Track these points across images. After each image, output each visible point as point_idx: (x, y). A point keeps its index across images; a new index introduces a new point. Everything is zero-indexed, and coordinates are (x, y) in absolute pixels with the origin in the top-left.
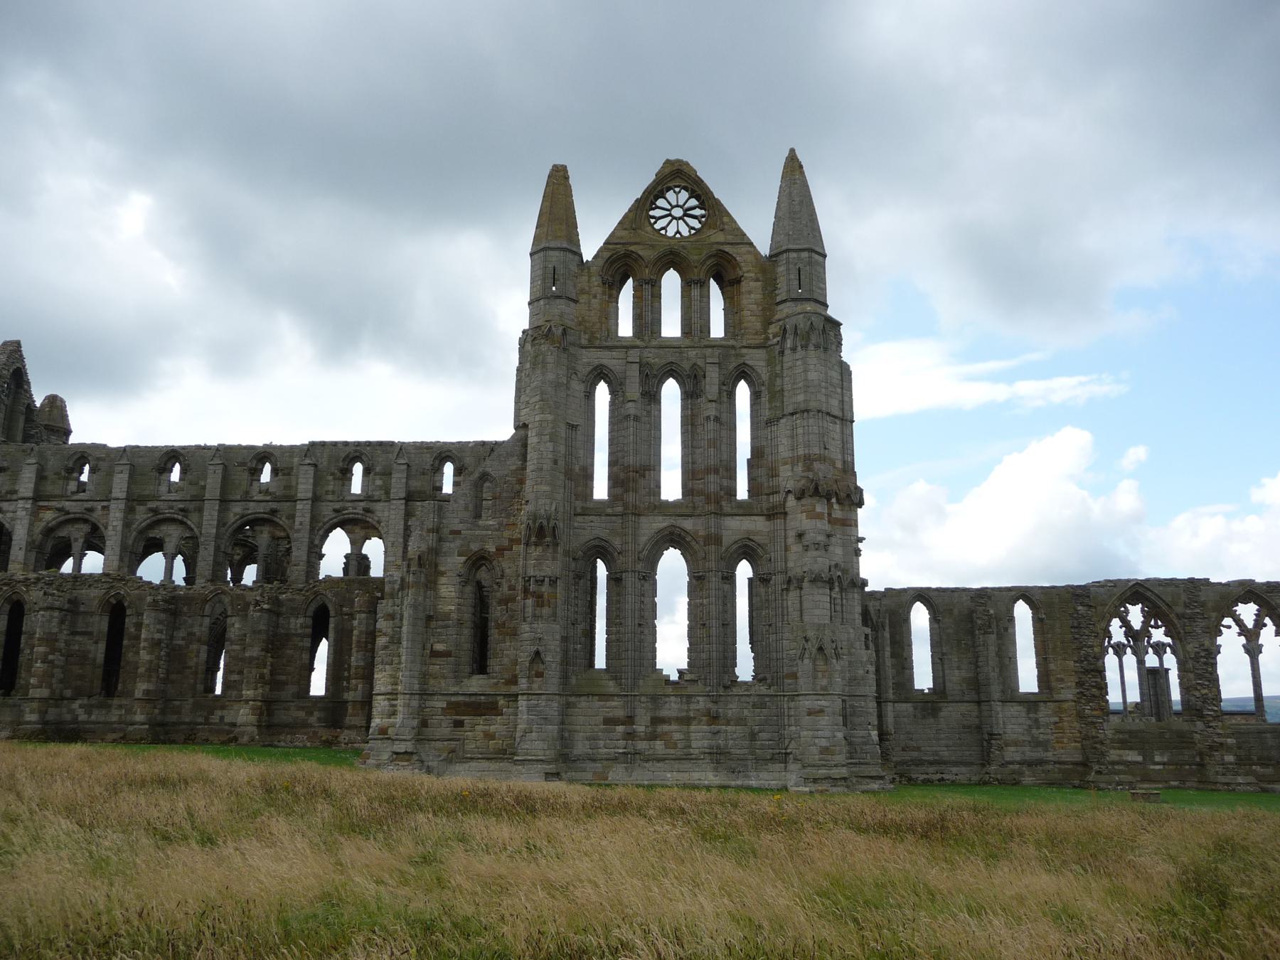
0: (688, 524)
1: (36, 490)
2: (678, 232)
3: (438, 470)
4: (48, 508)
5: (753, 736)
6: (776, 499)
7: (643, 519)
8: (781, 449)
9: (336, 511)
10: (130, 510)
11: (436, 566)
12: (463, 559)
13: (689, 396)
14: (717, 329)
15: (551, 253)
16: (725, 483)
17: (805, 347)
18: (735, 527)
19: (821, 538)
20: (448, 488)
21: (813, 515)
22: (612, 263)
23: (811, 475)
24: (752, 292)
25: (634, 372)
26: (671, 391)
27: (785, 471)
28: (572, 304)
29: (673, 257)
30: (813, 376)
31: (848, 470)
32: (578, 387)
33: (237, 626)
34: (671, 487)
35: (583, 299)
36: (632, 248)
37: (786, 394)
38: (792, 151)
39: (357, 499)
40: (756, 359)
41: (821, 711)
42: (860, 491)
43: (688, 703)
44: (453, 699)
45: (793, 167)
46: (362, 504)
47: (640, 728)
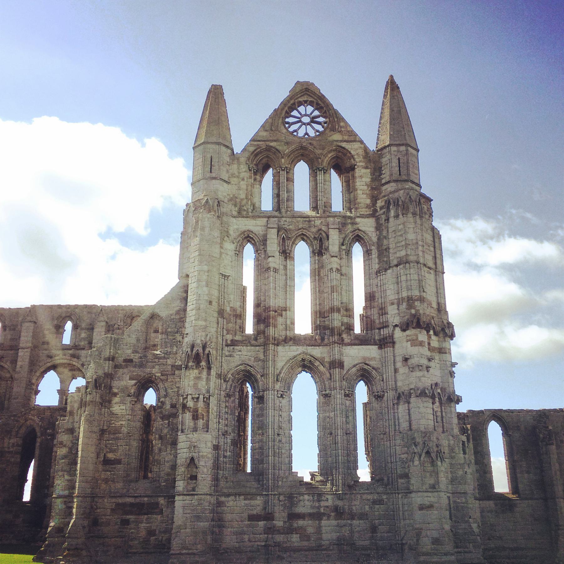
0: (317, 352)
2: (306, 134)
5: (374, 529)
6: (385, 332)
7: (280, 348)
8: (389, 292)
11: (111, 388)
12: (134, 382)
15: (209, 146)
16: (345, 320)
18: (353, 355)
19: (424, 362)
21: (415, 342)
22: (256, 155)
23: (413, 311)
24: (363, 177)
25: (273, 235)
27: (392, 310)
29: (304, 152)
30: (411, 236)
31: (441, 309)
32: (230, 247)
34: (303, 325)
35: (234, 180)
36: (272, 144)
37: (391, 251)
40: (367, 226)
41: (431, 507)
43: (319, 501)
44: (120, 501)
45: (392, 86)
47: (279, 523)
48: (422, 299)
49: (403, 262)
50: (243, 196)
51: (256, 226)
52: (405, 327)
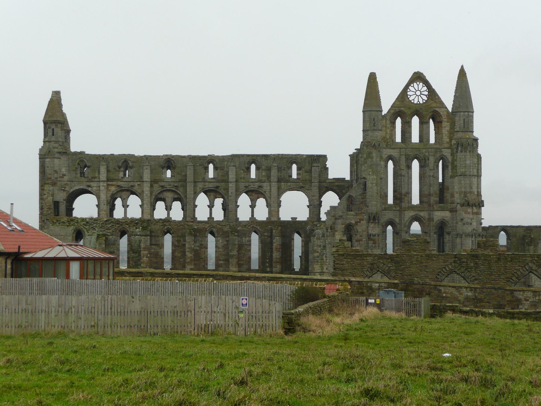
0: (422, 214)
1: (107, 177)
3: (290, 168)
4: (112, 185)
6: (454, 205)
7: (406, 212)
8: (456, 187)
9: (246, 187)
10: (152, 186)
13: (422, 167)
14: (432, 140)
17: (465, 152)
19: (469, 221)
20: (294, 176)
21: (466, 212)
24: (446, 126)
25: (403, 159)
26: (415, 164)
27: (457, 196)
28: (380, 132)
30: (468, 162)
31: (479, 194)
32: (383, 163)
33: (220, 241)
36: (402, 109)
38: (462, 66)
39: (253, 181)
40: (447, 153)
42: (483, 202)
45: (462, 74)
46: (257, 183)
48: (471, 192)
49: (464, 175)
50: (388, 137)
51: (395, 153)
52: (462, 205)
